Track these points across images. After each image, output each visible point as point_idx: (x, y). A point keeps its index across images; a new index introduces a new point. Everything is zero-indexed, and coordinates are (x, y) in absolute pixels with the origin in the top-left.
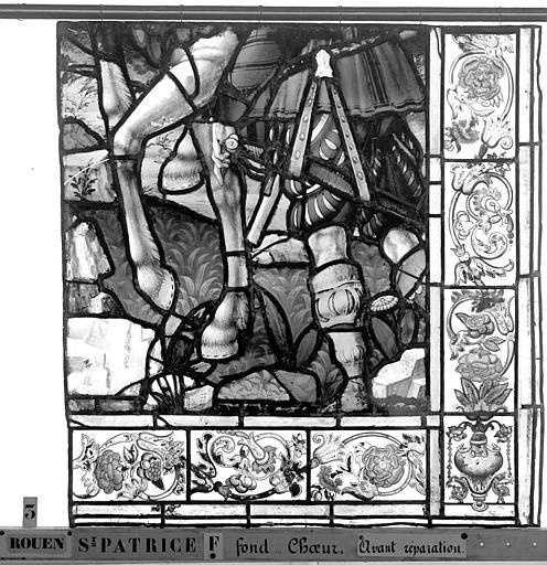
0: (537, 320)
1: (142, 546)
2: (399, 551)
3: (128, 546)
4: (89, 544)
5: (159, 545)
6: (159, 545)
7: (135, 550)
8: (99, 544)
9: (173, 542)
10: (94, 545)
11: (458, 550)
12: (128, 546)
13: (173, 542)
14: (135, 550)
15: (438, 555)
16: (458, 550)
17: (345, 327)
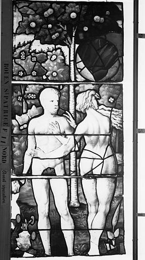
0: (78, 164)
1: (6, 109)
2: (2, 183)
3: (6, 105)
4: (7, 92)
5: (6, 114)
6: (6, 114)
7: (5, 106)
8: (7, 95)
9: (6, 119)
10: (6, 94)
11: (4, 202)
12: (6, 105)
13: (6, 119)
14: (5, 106)
15: (2, 194)
16: (4, 202)
17: (52, 198)
